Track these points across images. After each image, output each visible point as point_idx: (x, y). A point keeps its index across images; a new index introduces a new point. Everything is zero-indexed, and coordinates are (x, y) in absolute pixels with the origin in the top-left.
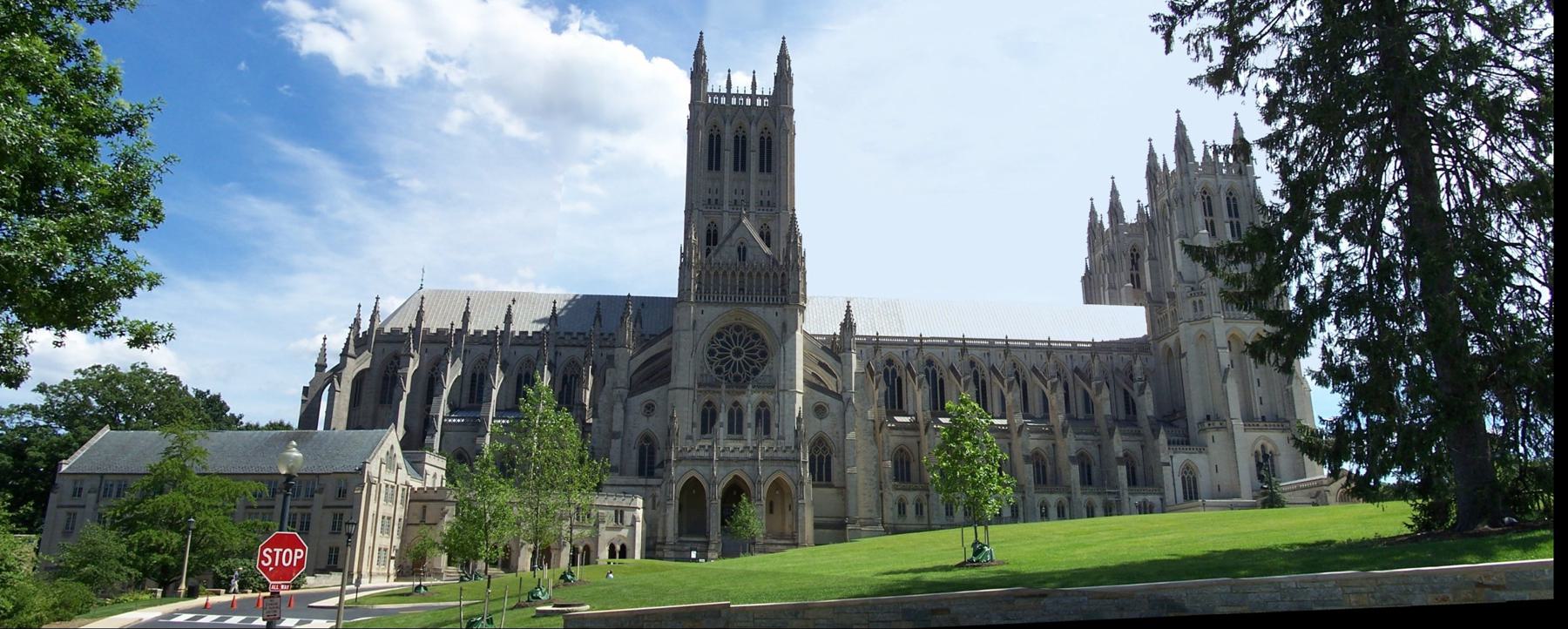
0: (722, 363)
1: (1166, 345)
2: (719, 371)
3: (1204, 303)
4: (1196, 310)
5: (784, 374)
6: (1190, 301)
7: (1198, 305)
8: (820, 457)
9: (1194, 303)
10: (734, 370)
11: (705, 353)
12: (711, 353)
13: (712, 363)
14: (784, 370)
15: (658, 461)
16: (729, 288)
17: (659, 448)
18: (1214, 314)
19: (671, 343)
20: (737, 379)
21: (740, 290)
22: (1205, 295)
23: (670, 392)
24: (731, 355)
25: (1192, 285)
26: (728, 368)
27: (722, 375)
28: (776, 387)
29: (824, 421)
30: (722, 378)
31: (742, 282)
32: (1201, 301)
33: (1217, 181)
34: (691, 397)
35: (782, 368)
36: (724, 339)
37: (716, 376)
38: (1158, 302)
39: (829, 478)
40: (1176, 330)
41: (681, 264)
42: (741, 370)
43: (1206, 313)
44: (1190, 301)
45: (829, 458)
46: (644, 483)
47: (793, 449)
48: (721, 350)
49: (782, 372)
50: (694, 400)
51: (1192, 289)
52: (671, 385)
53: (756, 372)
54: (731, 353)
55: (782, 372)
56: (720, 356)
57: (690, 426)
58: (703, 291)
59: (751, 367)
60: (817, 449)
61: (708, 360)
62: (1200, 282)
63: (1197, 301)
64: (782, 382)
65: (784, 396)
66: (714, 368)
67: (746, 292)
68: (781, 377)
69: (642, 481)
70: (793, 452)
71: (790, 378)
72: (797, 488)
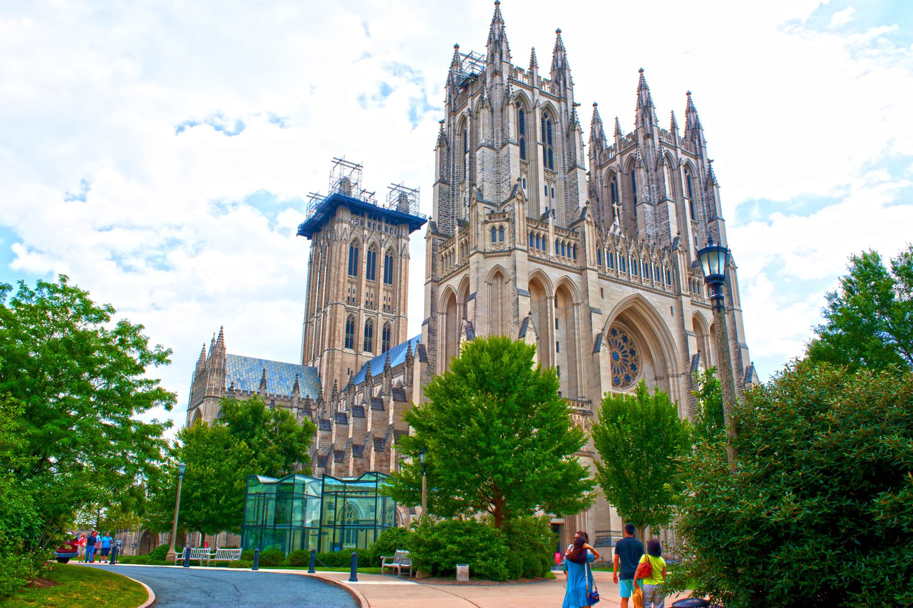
1: (449, 289)
3: (506, 231)
4: (494, 240)
6: (488, 226)
7: (497, 233)
9: (493, 229)
18: (518, 246)
22: (508, 220)
25: (492, 208)
32: (501, 227)
33: (533, 94)
38: (442, 235)
40: (466, 265)
43: (507, 244)
44: (488, 226)
51: (493, 212)
62: (503, 204)
63: (497, 228)
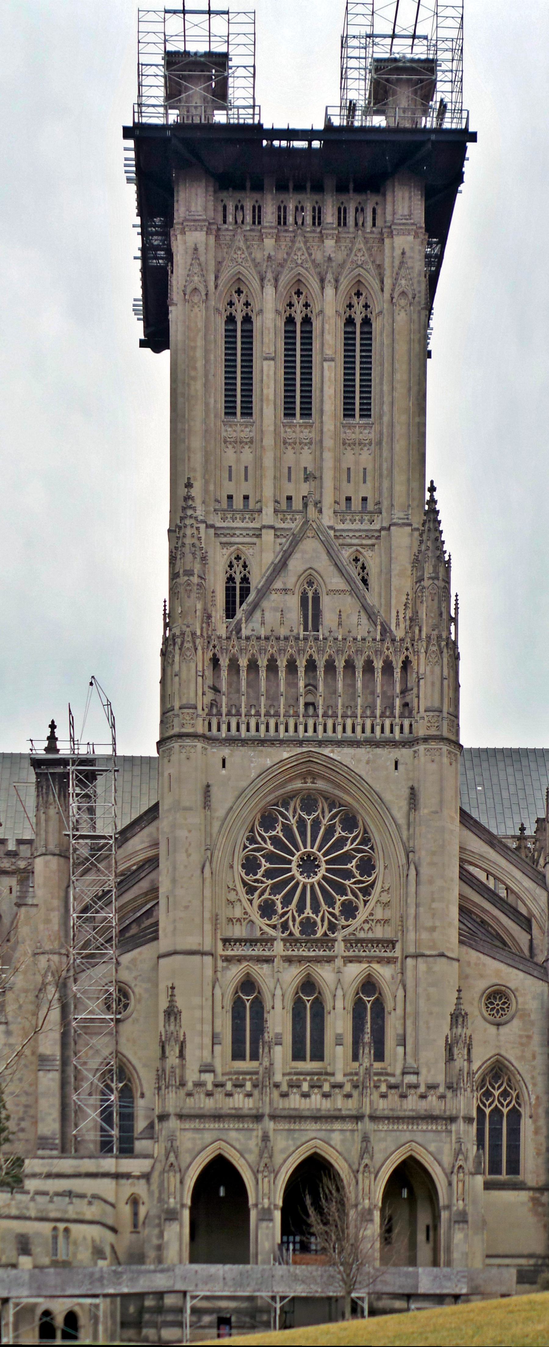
0: (276, 889)
2: (267, 910)
5: (416, 917)
8: (496, 1111)
10: (301, 908)
11: (239, 870)
12: (250, 865)
13: (251, 890)
14: (417, 905)
15: (140, 1124)
16: (282, 700)
17: (142, 1096)
19: (156, 845)
20: (308, 926)
21: (307, 705)
23: (162, 961)
24: (295, 871)
26: (287, 901)
27: (275, 920)
28: (398, 946)
29: (504, 1030)
30: (274, 927)
31: (311, 687)
34: (209, 972)
35: (411, 900)
36: (278, 831)
37: (261, 922)
39: (514, 1168)
41: (165, 640)
42: (316, 908)
45: (515, 1115)
46: (113, 1170)
47: (442, 1089)
48: (270, 857)
49: (412, 911)
50: (215, 981)
52: (164, 944)
53: (350, 911)
54: (294, 866)
55: (412, 911)
56: (269, 874)
57: (208, 1041)
58: (224, 710)
59: (340, 899)
60: (488, 1094)
61: (245, 883)
64: (411, 936)
65: (416, 967)
66: (256, 902)
67: (320, 712)
68: (411, 922)
69: (109, 1164)
70: (442, 1097)
71: (429, 924)
72: (450, 1184)
